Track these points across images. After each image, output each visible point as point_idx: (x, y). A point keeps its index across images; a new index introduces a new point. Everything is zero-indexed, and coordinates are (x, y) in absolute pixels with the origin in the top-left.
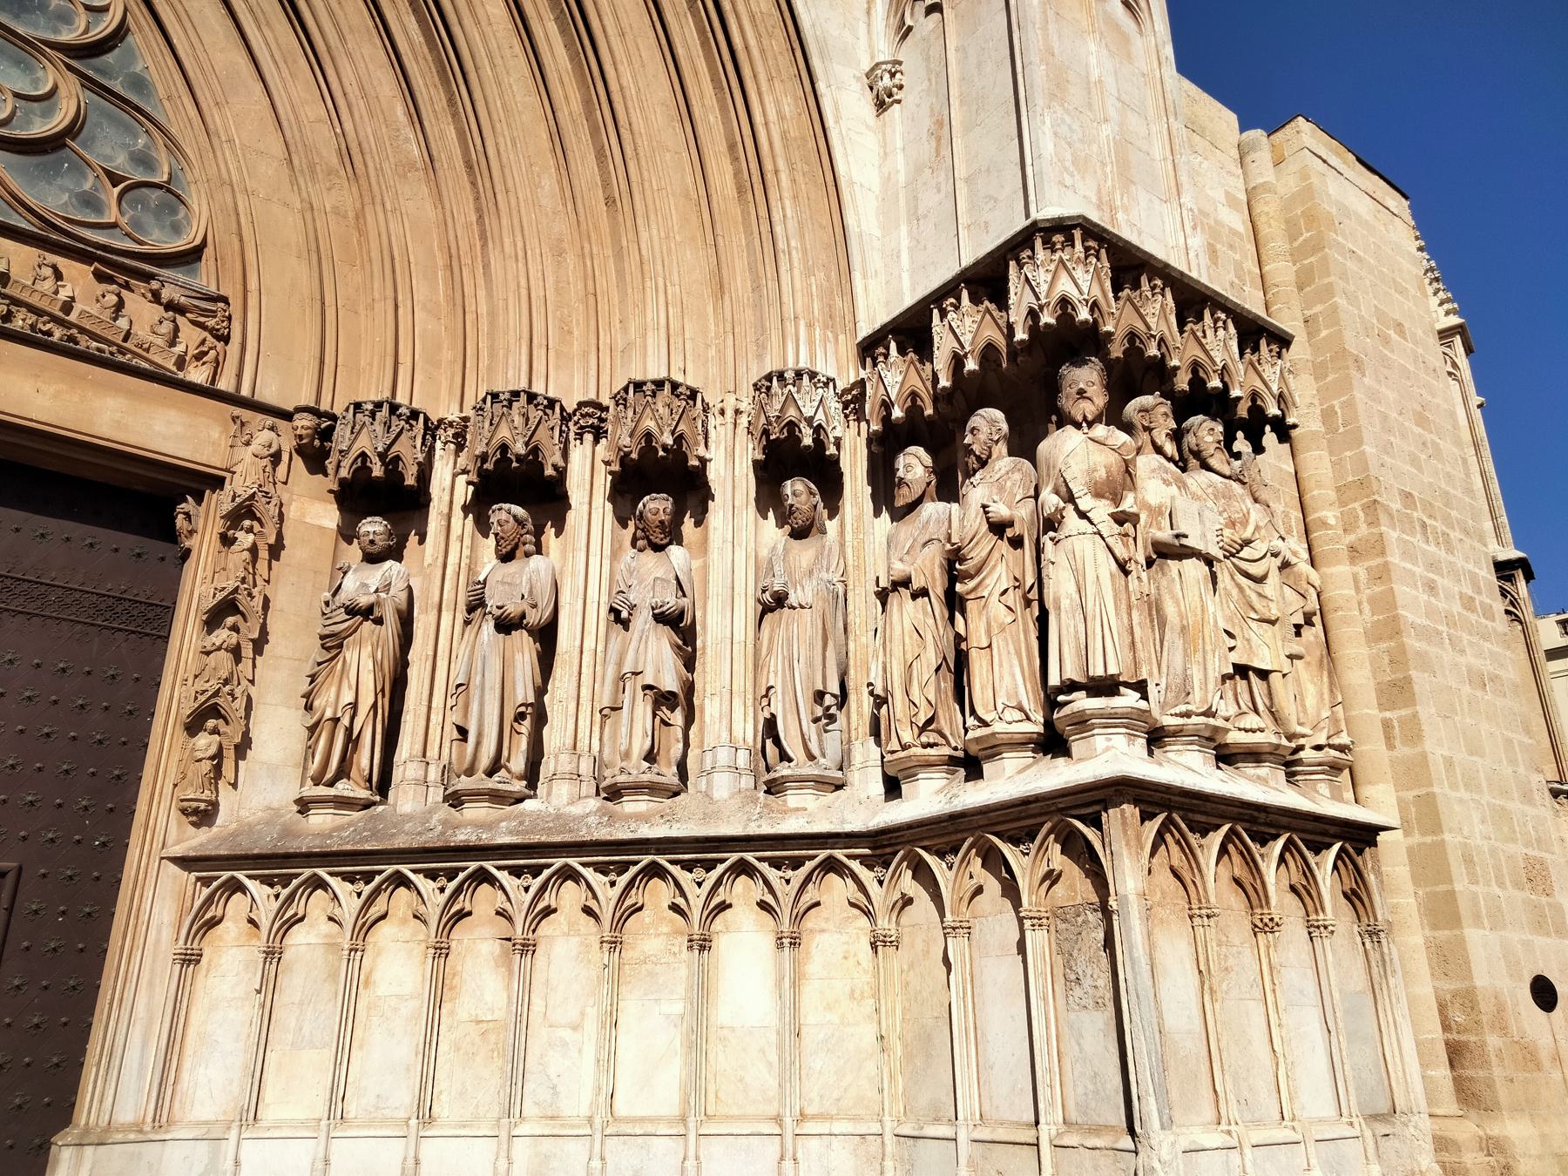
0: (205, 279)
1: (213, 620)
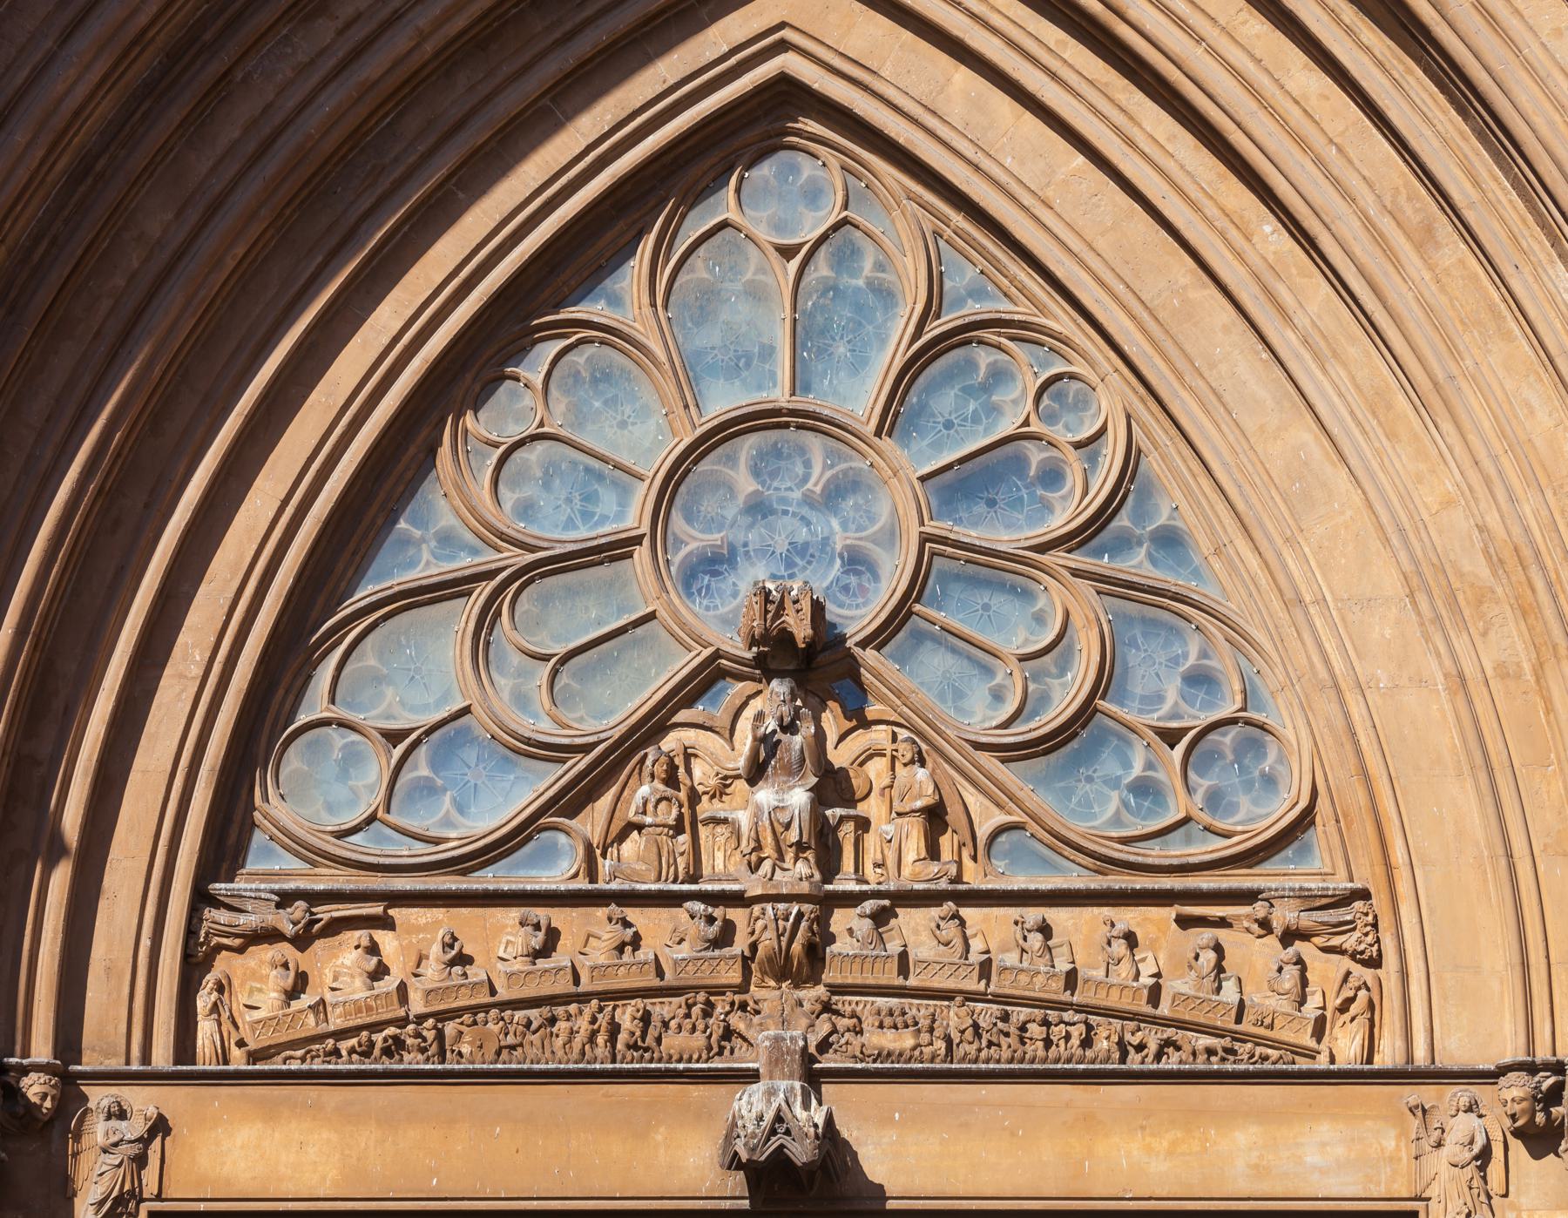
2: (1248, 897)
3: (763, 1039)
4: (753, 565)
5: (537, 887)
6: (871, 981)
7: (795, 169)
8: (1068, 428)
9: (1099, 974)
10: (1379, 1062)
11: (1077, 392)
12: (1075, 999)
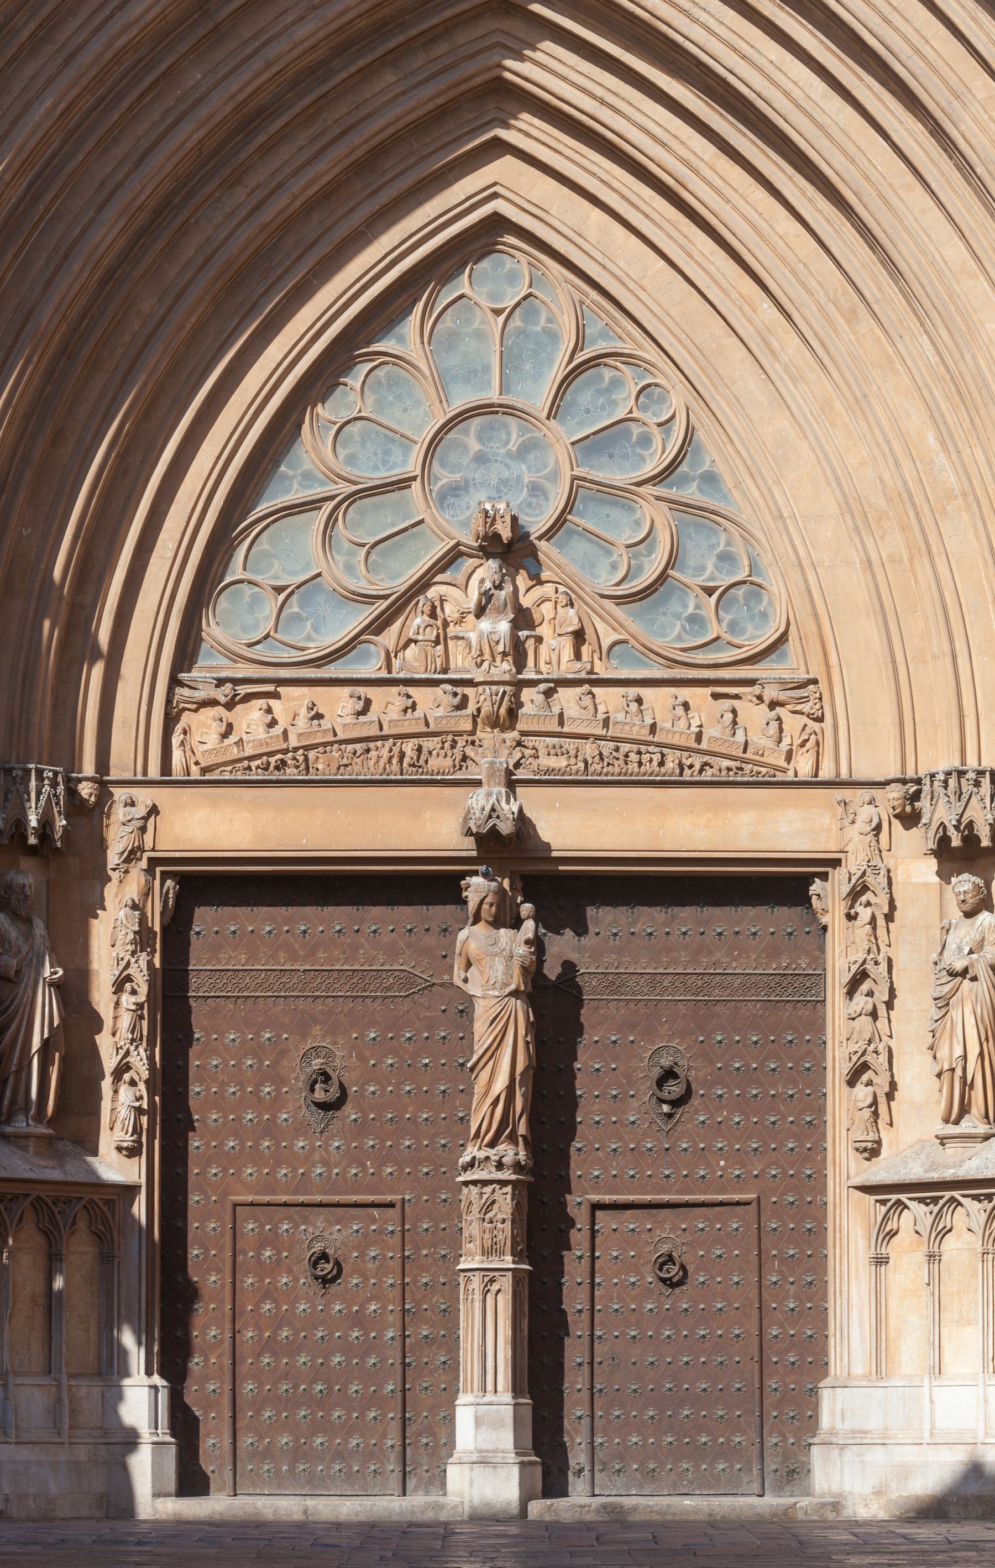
0: (795, 662)
1: (852, 988)
2: (751, 682)
3: (484, 762)
4: (478, 491)
5: (359, 676)
6: (543, 729)
7: (502, 264)
8: (654, 414)
9: (668, 725)
11: (659, 394)
12: (655, 740)
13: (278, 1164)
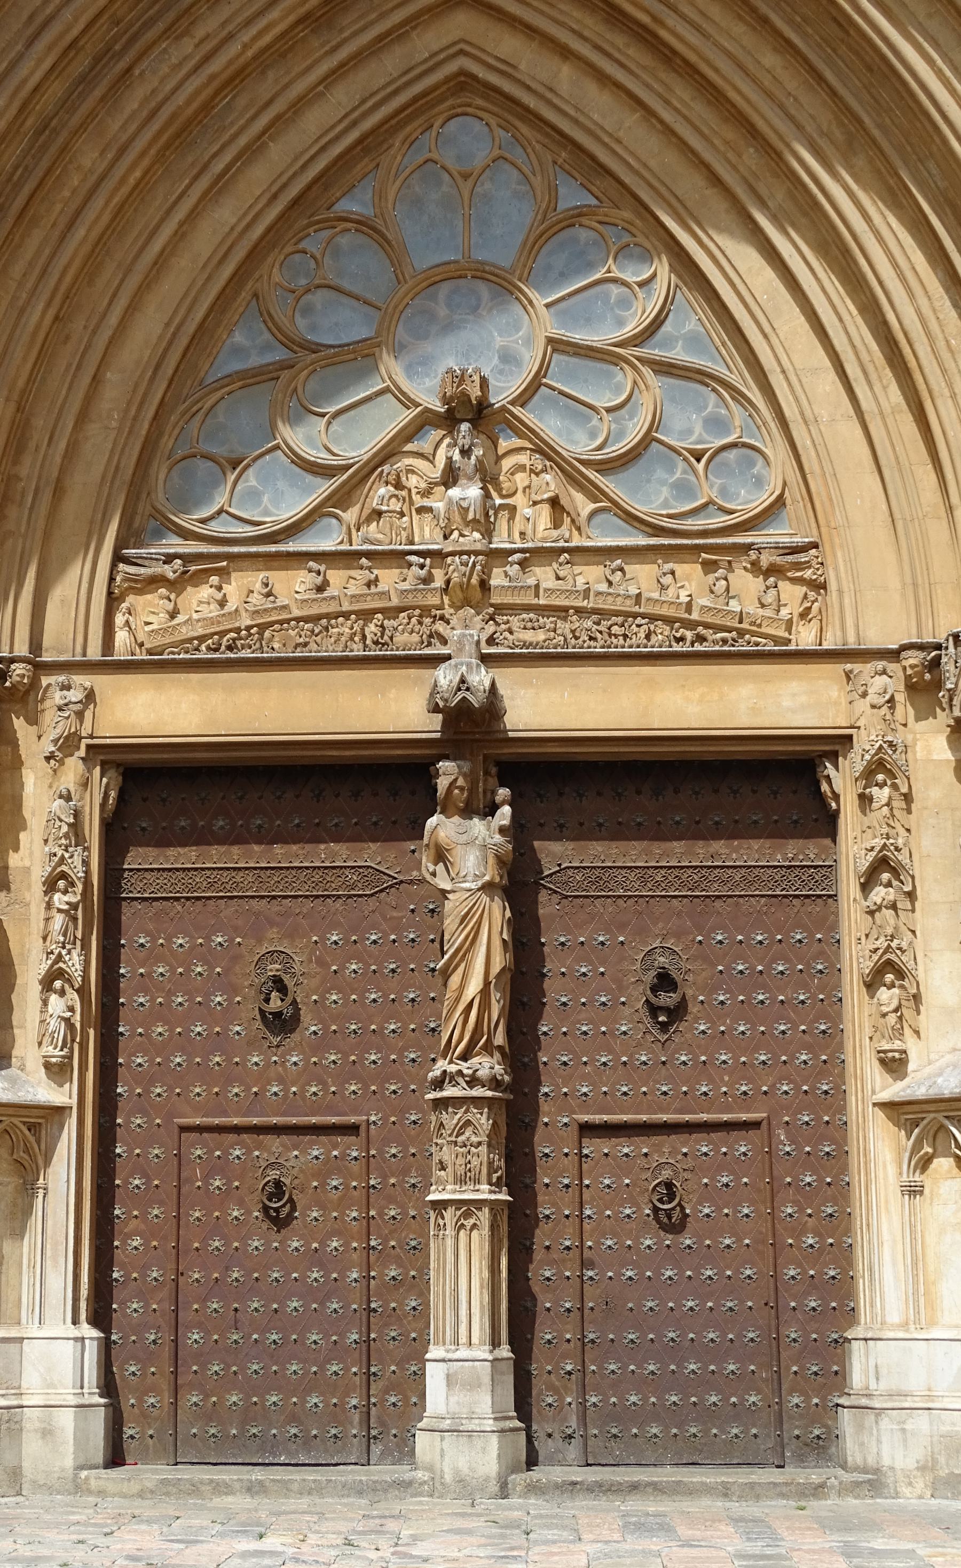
9: (655, 595)
10: (826, 646)
12: (642, 610)
13: (229, 1082)
